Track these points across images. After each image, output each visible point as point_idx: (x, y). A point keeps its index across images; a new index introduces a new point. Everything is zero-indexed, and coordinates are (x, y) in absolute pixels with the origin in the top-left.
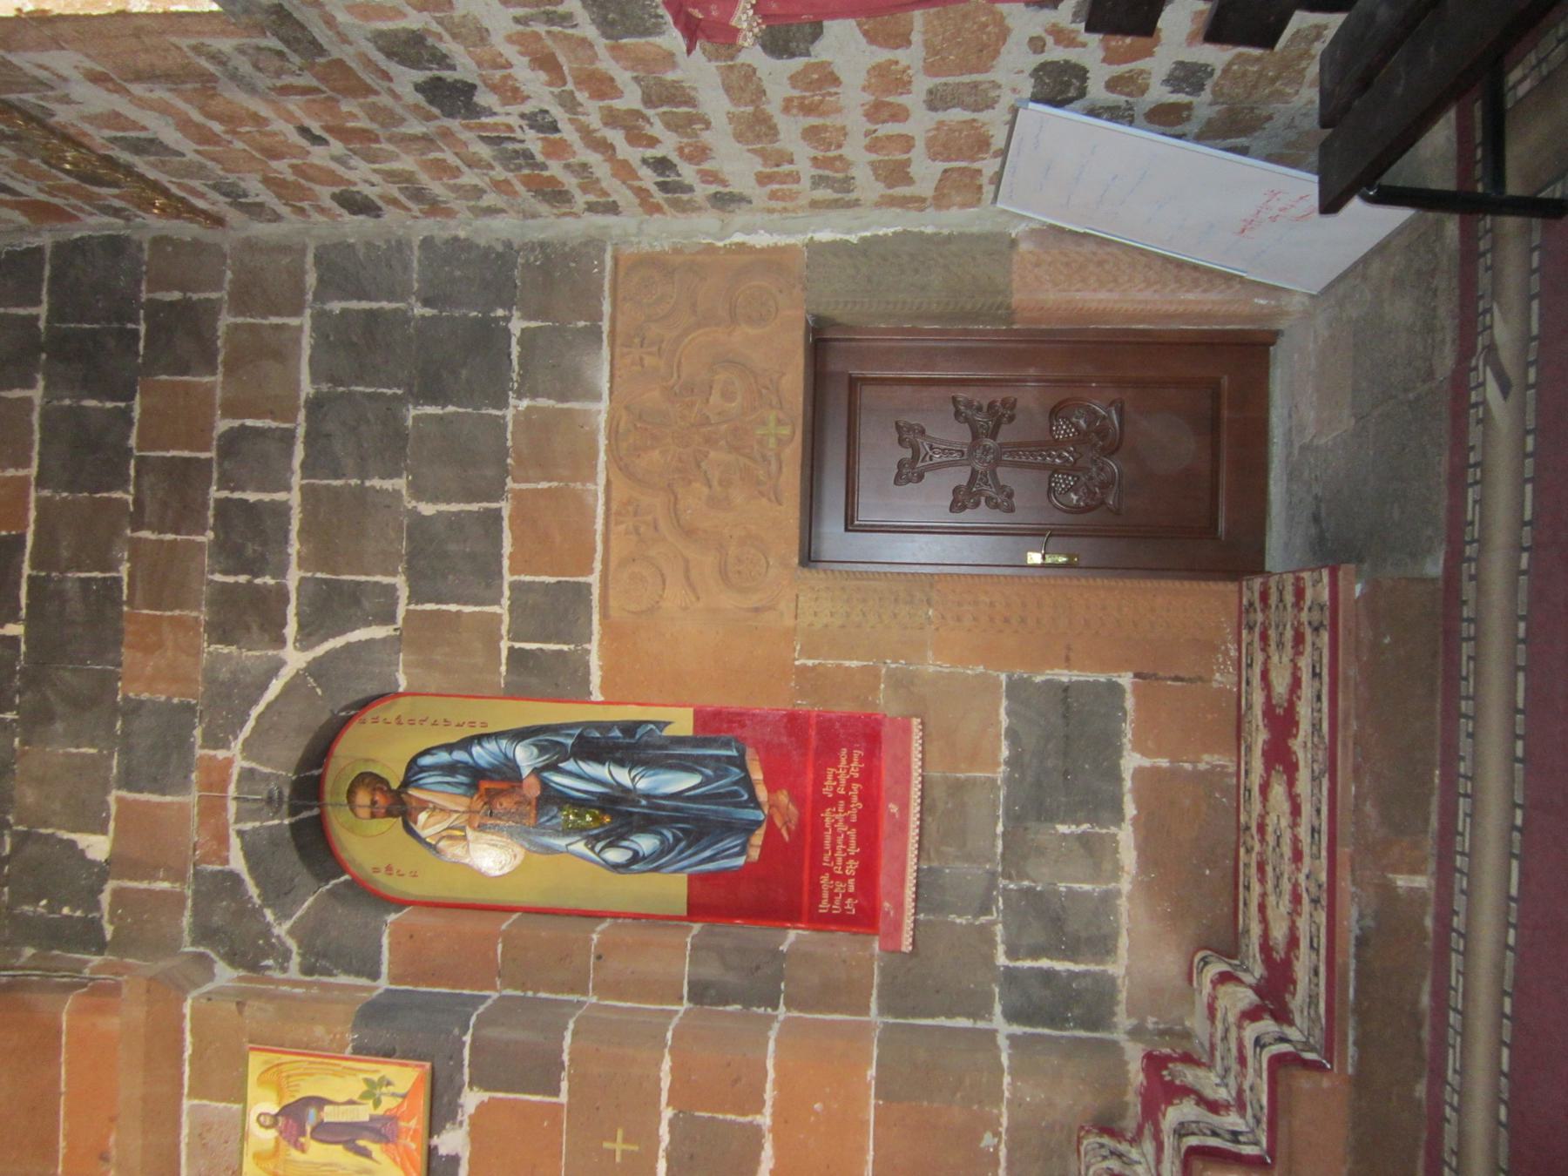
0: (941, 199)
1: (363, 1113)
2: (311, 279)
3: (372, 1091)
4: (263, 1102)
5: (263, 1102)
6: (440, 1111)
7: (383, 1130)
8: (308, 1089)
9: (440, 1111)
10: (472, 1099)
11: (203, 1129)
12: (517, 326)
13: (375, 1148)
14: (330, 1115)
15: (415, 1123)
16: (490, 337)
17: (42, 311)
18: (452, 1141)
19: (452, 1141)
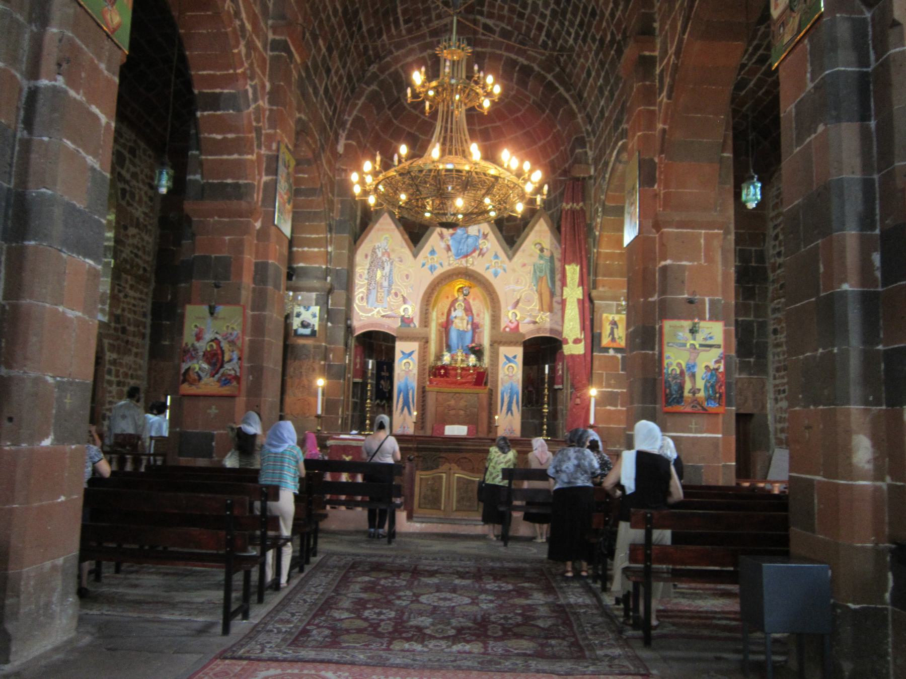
0: (777, 438)
1: (616, 336)
2: (760, 320)
3: (620, 338)
4: (617, 318)
5: (617, 318)
6: (617, 350)
7: (613, 340)
8: (620, 326)
9: (617, 350)
10: (619, 356)
11: (611, 305)
12: (752, 360)
13: (610, 338)
14: (615, 330)
15: (615, 345)
16: (750, 355)
17: (753, 264)
18: (611, 352)
19: (611, 352)
